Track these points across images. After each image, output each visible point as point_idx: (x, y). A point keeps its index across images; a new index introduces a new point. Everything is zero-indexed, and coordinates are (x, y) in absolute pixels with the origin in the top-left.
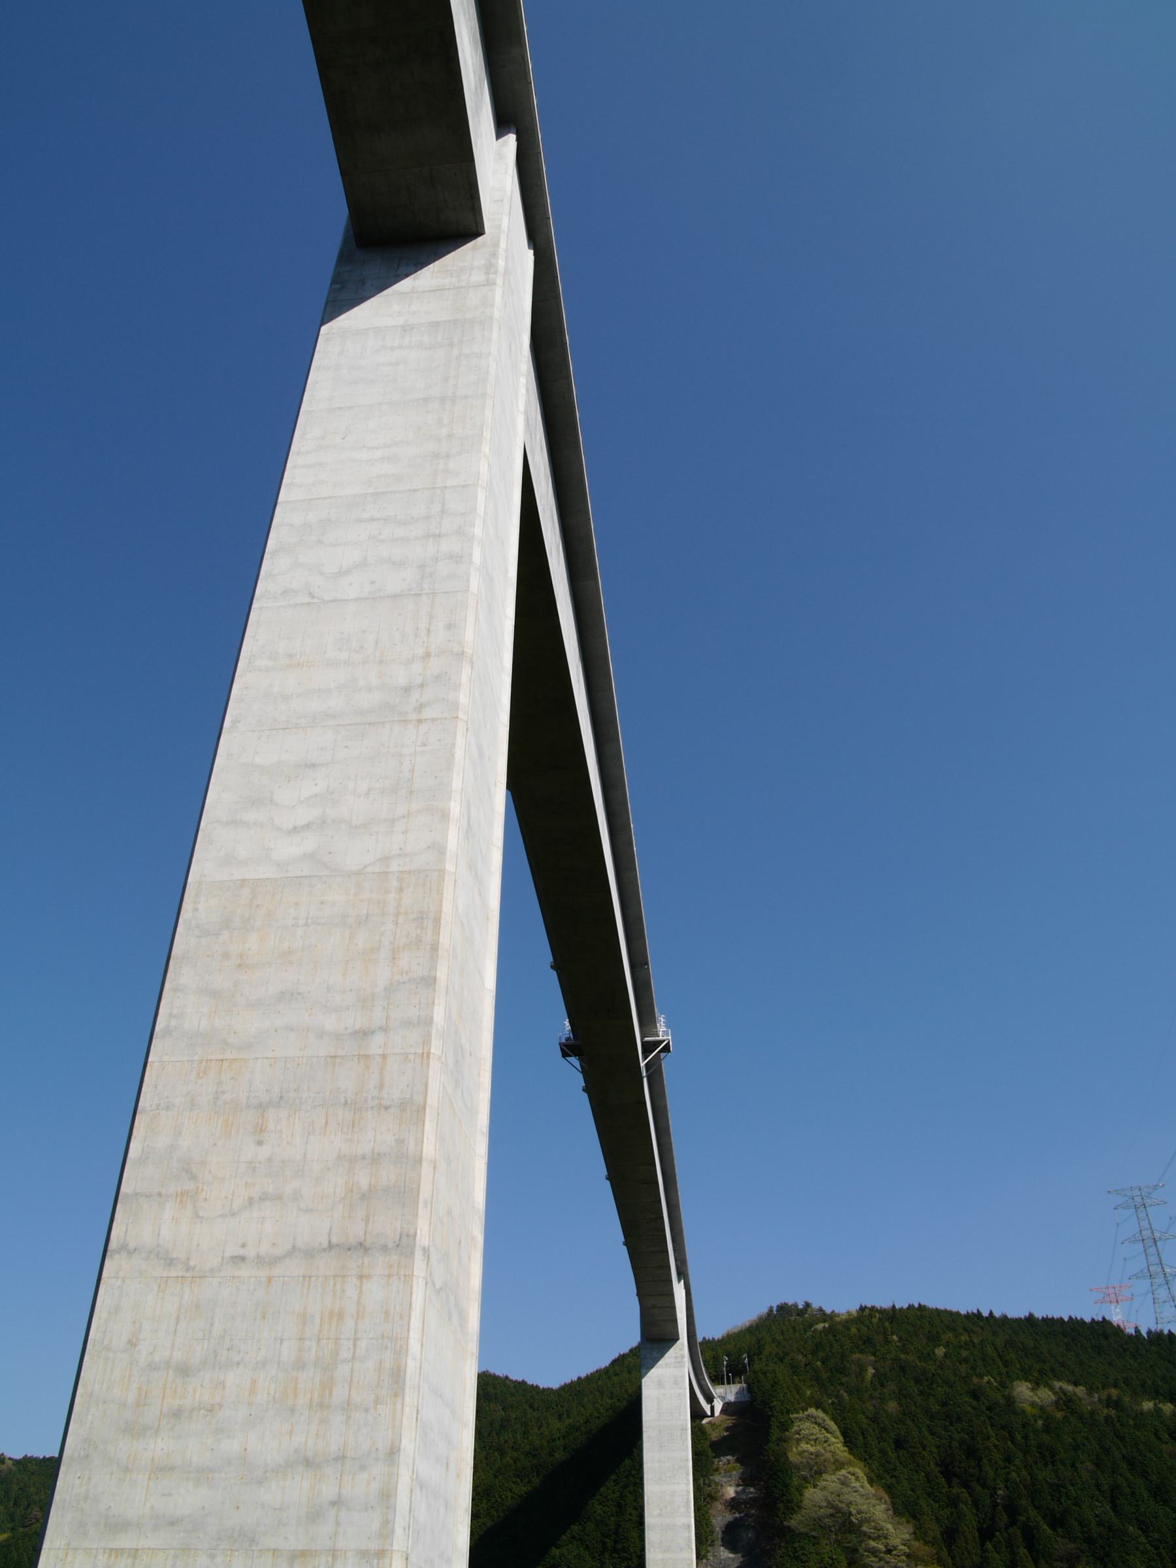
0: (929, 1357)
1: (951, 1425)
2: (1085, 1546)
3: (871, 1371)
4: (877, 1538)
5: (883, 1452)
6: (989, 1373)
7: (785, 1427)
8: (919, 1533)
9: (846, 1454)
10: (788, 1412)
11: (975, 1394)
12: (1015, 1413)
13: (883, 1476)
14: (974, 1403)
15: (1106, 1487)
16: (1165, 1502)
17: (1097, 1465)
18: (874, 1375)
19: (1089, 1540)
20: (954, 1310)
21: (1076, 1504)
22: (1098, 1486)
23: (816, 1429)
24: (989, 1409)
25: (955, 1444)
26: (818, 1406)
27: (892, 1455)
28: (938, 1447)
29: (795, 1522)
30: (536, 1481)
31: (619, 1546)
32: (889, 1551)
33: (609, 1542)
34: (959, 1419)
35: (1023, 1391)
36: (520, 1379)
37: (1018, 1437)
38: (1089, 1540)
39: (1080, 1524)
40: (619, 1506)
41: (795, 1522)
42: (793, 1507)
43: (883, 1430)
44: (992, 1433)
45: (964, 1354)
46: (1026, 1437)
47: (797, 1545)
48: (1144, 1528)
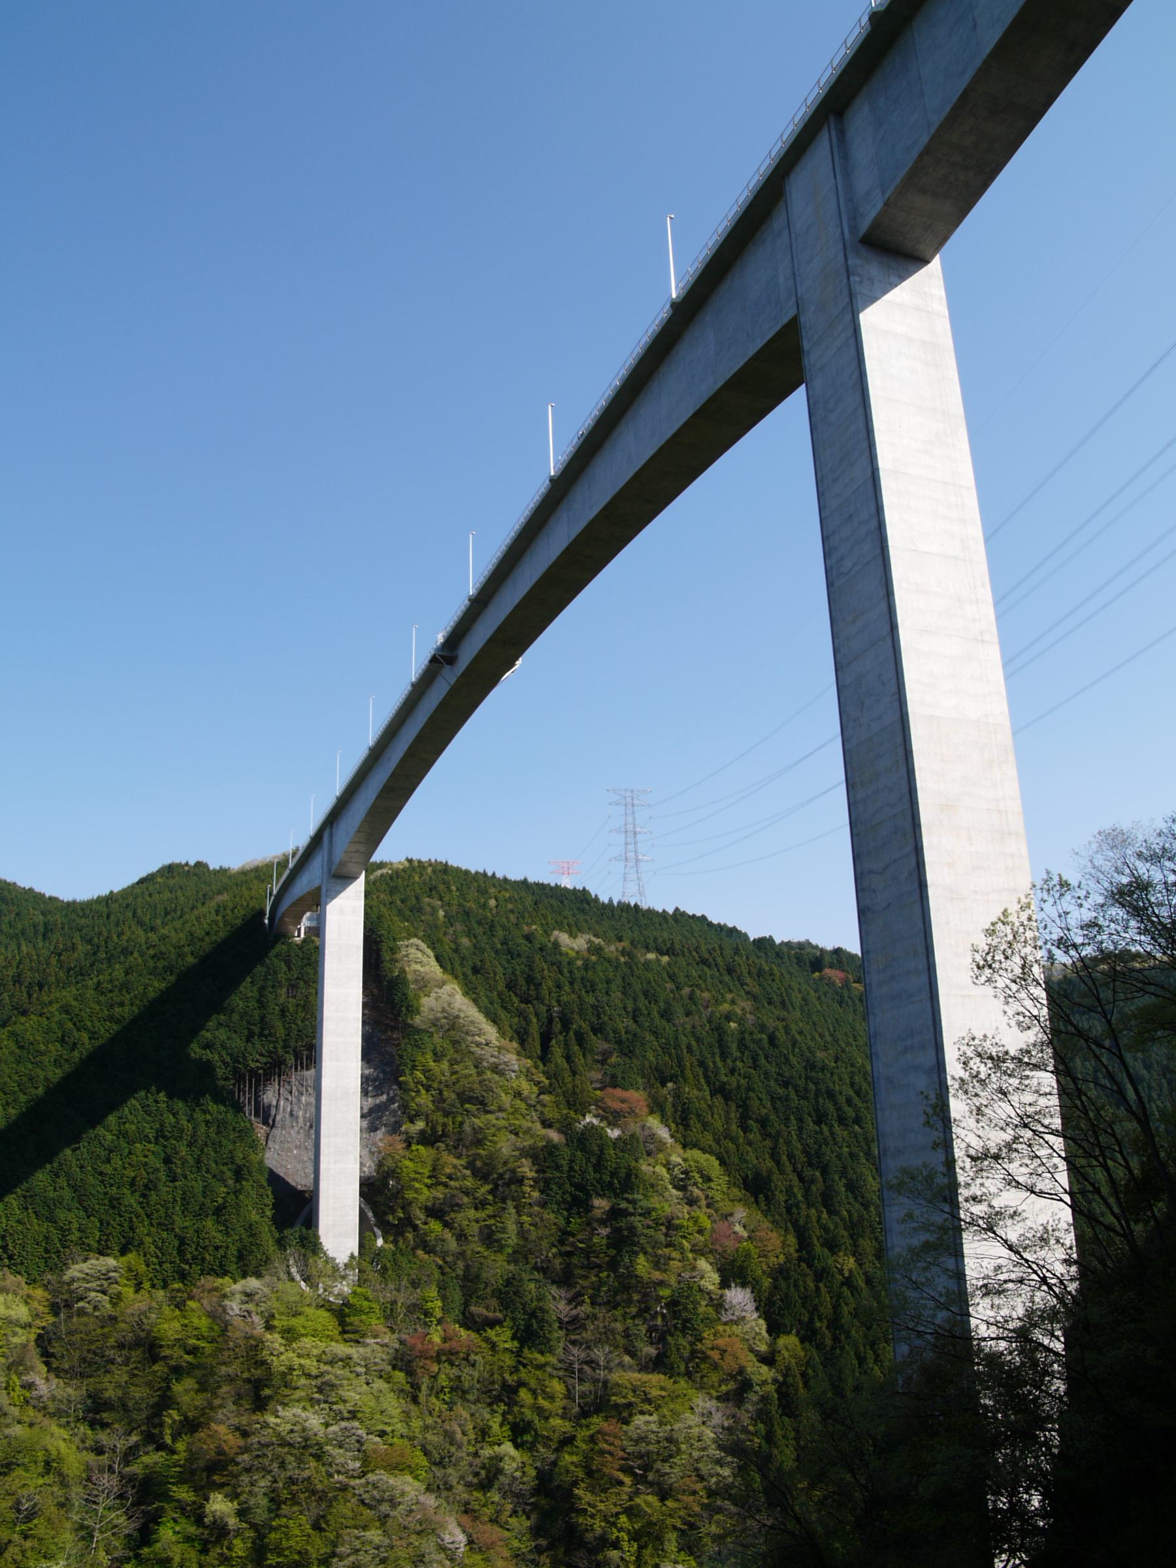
0: (484, 906)
1: (512, 959)
2: (616, 1046)
3: (441, 913)
4: (479, 1035)
5: (464, 974)
6: (535, 924)
7: (394, 950)
8: (502, 1033)
9: (441, 975)
10: (394, 939)
11: (528, 938)
12: (561, 954)
13: (470, 991)
14: (529, 945)
15: (629, 1009)
16: (669, 1021)
17: (623, 994)
18: (445, 916)
19: (619, 1042)
20: (546, 882)
21: (610, 1019)
22: (625, 1008)
23: (419, 955)
24: (541, 949)
25: (518, 972)
26: (416, 936)
27: (471, 977)
28: (504, 974)
29: (417, 1020)
30: (173, 978)
31: (266, 1032)
32: (487, 1044)
33: (256, 1030)
34: (519, 955)
35: (564, 938)
36: (802, 939)
37: (565, 971)
38: (619, 1042)
39: (614, 1031)
40: (259, 1001)
41: (417, 1020)
42: (413, 1010)
43: (463, 959)
44: (546, 967)
45: (510, 906)
46: (571, 972)
47: (416, 1037)
48: (655, 1033)
